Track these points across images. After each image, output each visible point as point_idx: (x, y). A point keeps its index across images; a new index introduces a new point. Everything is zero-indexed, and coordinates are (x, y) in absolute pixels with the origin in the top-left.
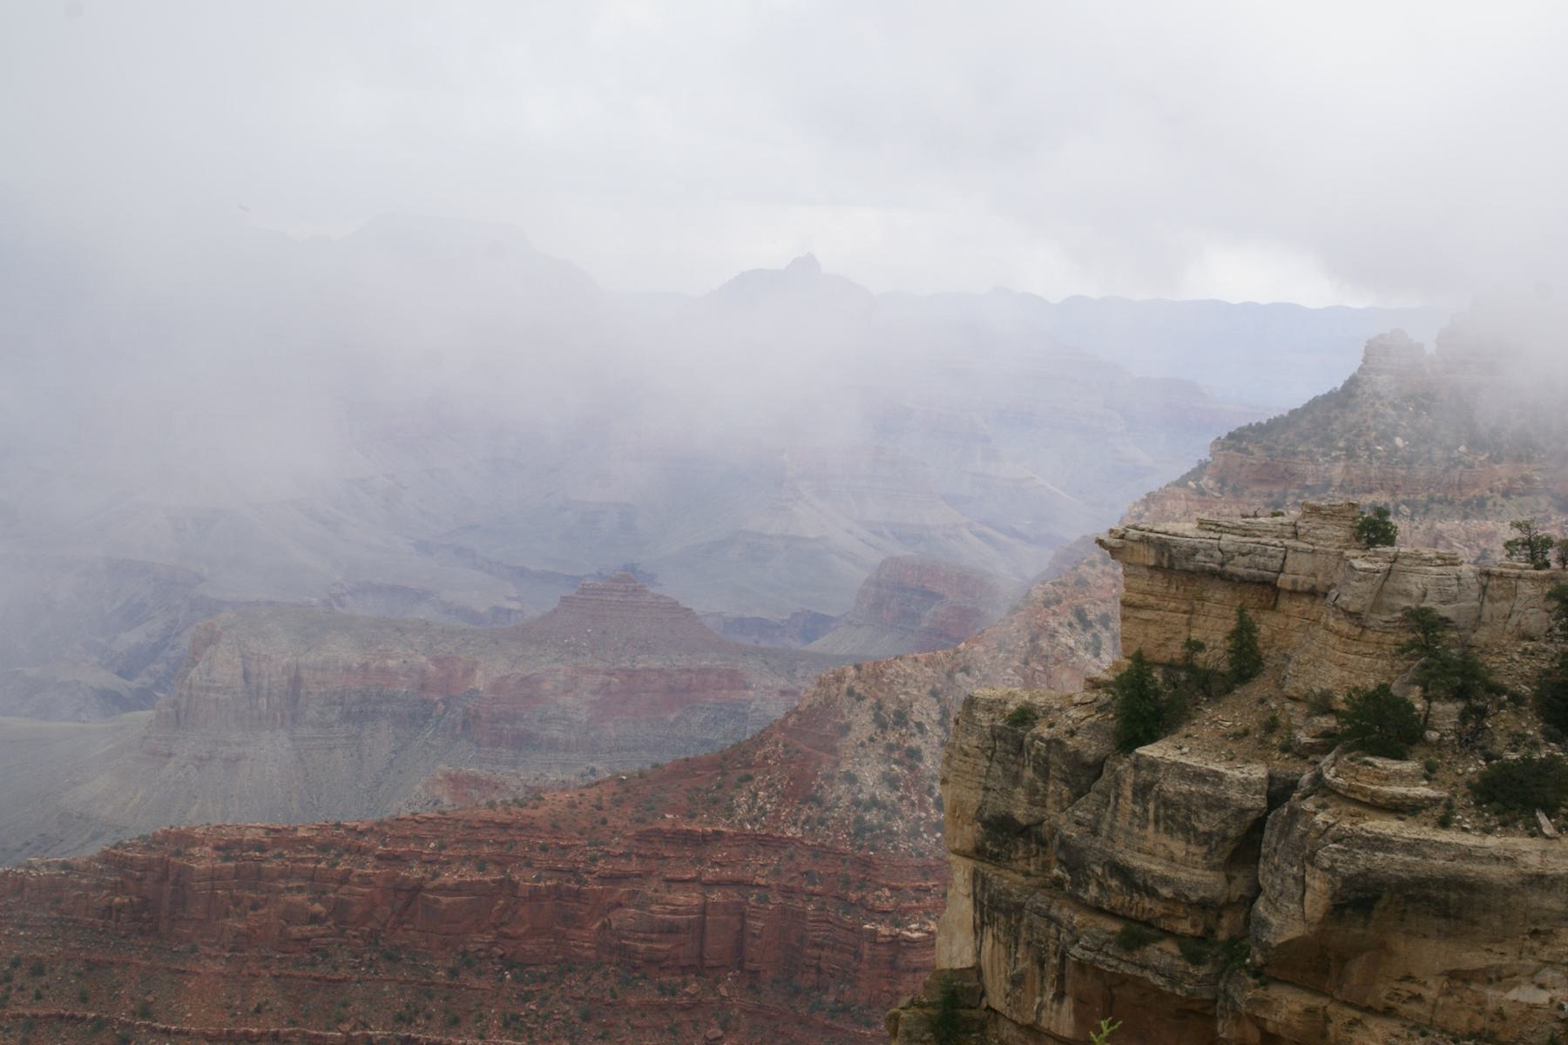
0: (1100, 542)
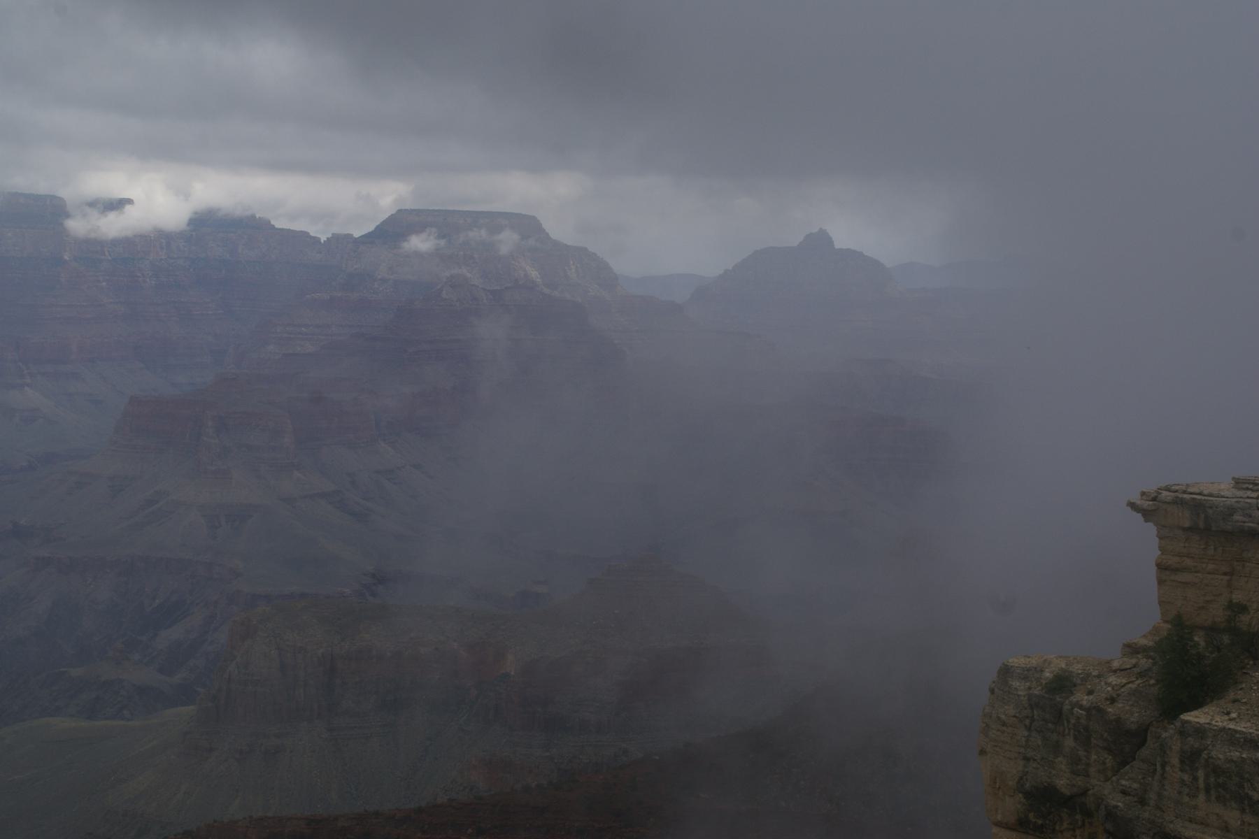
0: (1132, 505)
